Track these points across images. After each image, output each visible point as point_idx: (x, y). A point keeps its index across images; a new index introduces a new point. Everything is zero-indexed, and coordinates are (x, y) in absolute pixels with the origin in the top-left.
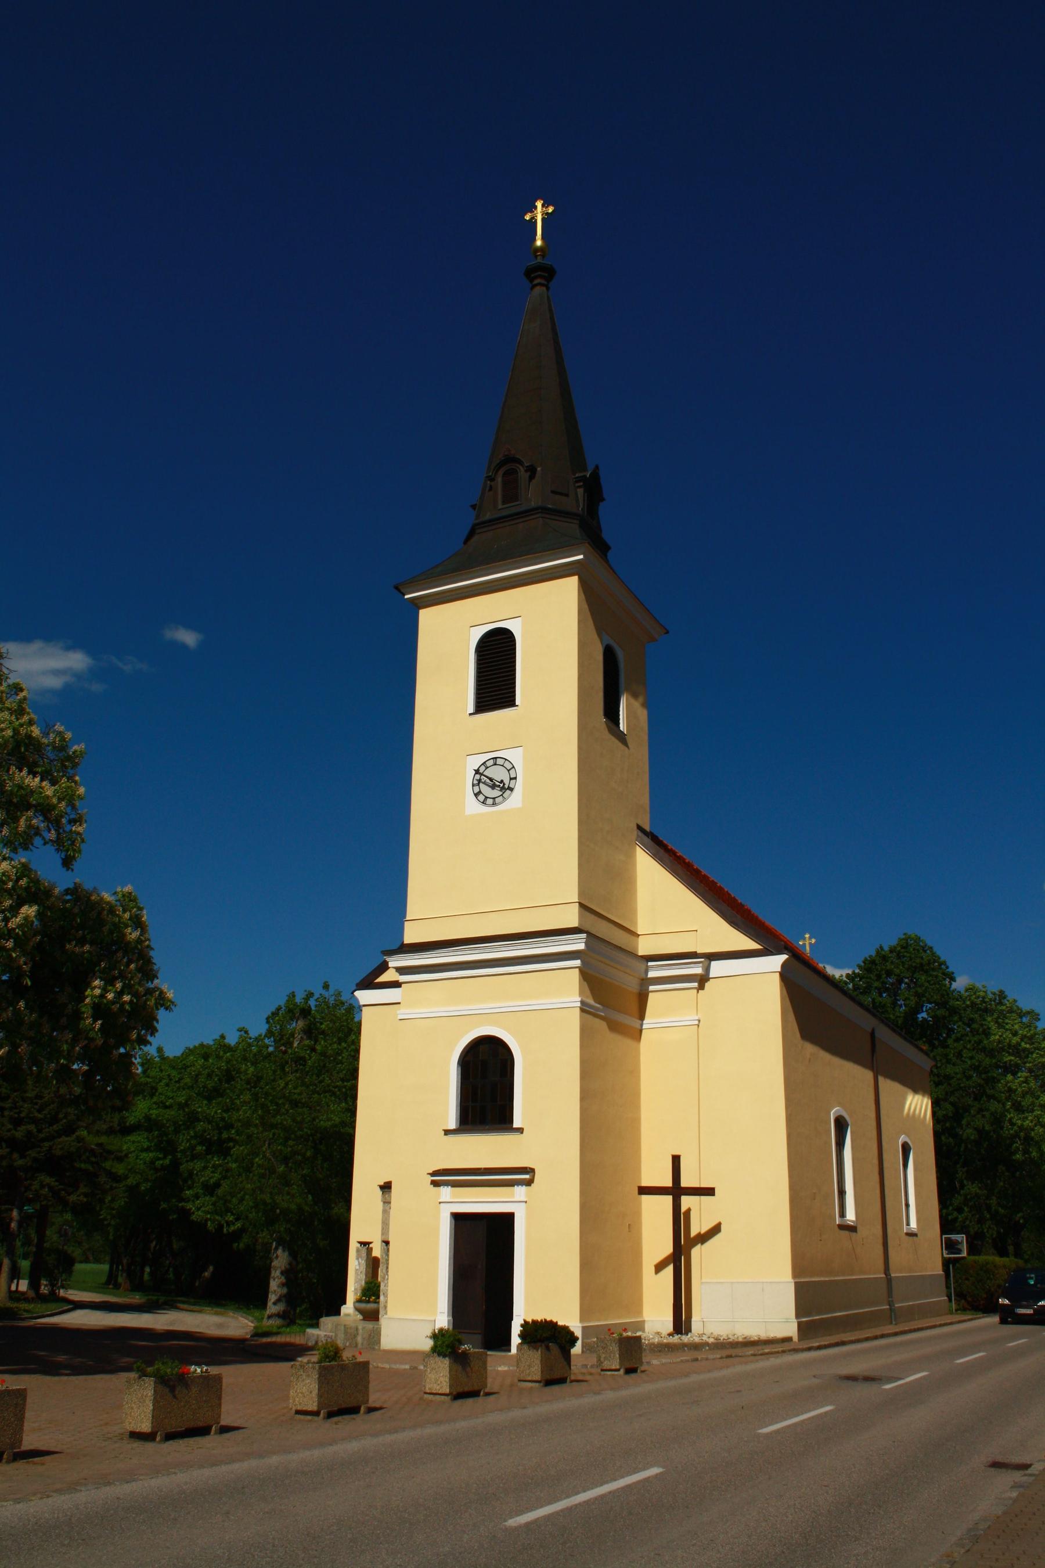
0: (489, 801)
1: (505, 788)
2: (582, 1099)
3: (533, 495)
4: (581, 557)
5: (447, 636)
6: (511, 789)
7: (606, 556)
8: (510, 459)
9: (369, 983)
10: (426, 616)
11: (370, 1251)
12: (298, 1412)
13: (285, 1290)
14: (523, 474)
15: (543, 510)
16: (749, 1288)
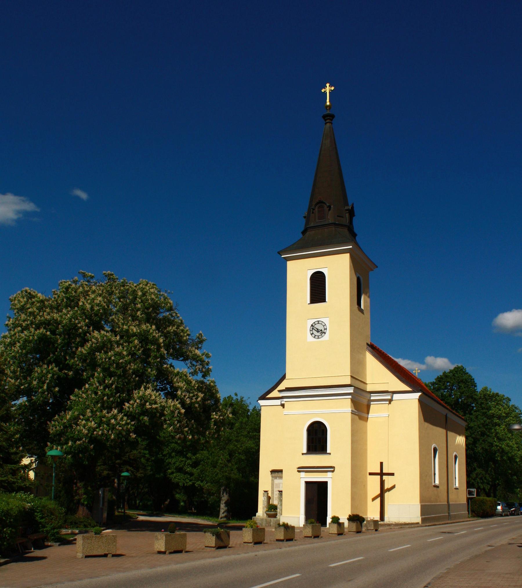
0: (317, 337)
1: (323, 332)
2: (352, 443)
3: (330, 218)
4: (351, 247)
5: (298, 273)
6: (325, 333)
7: (355, 238)
8: (320, 202)
9: (264, 397)
10: (290, 264)
11: (268, 494)
12: (305, 537)
13: (226, 508)
14: (325, 207)
15: (335, 224)
16: (404, 506)
